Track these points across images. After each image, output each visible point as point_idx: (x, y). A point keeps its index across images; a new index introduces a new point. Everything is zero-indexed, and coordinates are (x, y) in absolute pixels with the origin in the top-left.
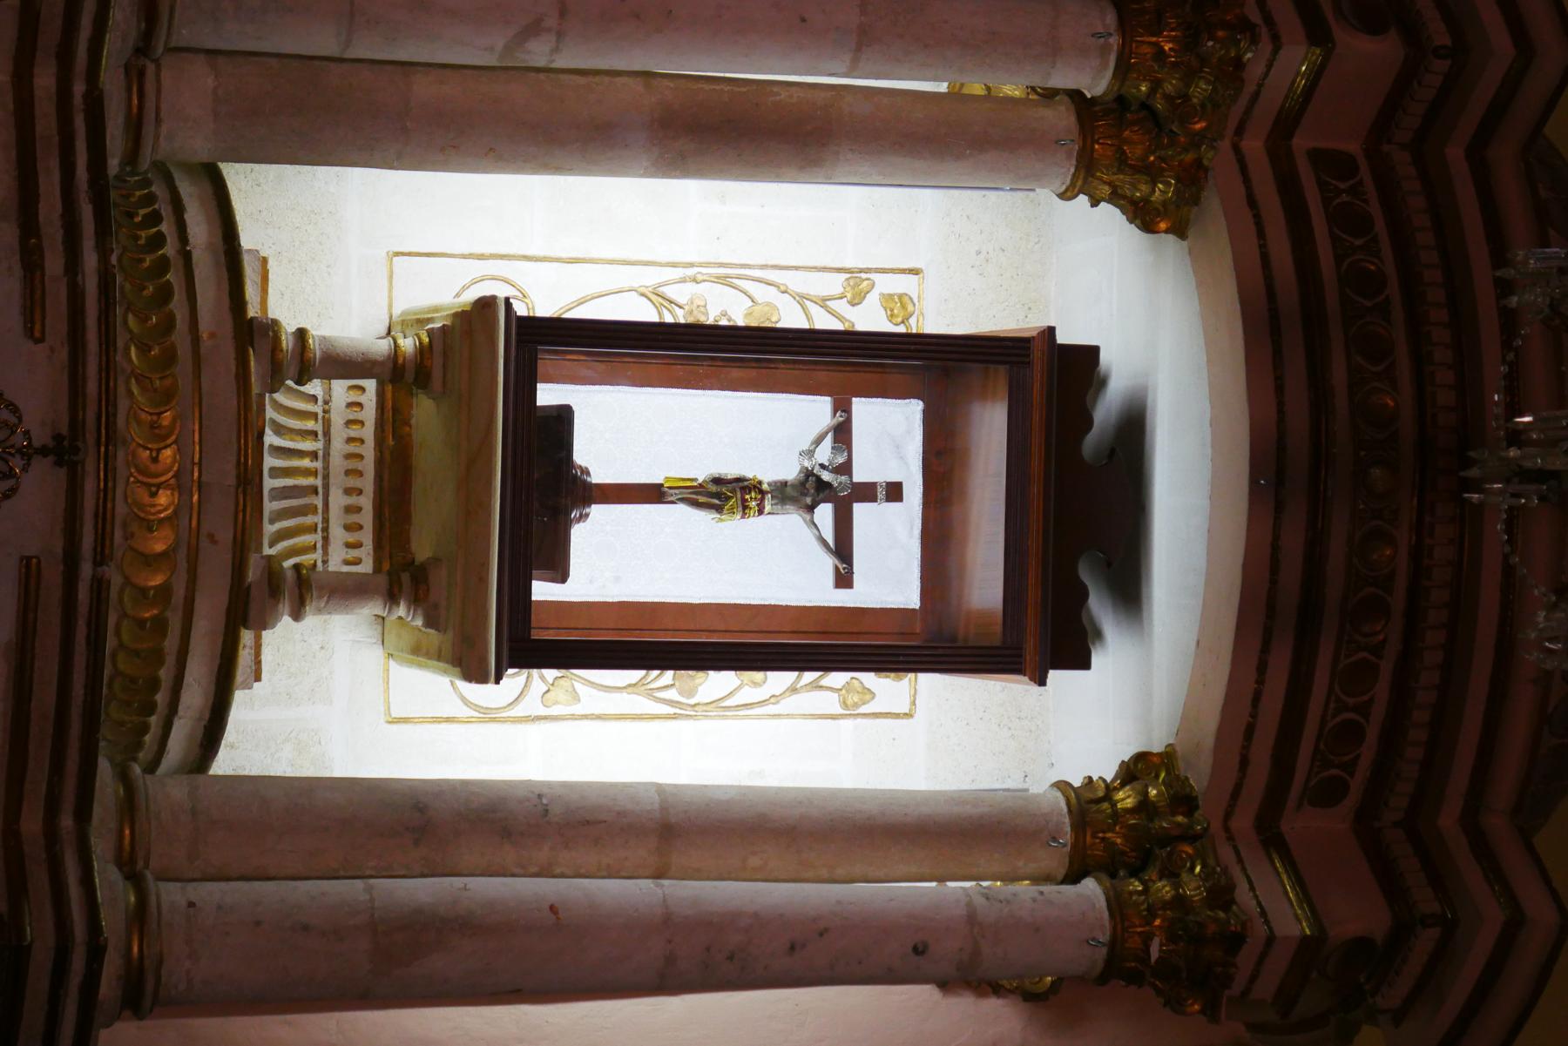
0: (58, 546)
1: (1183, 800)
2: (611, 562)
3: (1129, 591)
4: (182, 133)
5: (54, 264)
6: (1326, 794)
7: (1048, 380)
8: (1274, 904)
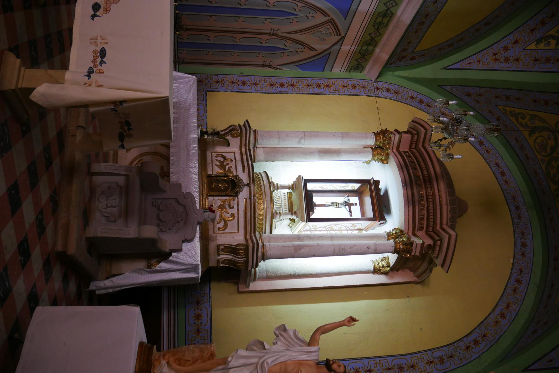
0: (249, 197)
1: (401, 231)
3: (389, 212)
5: (246, 165)
6: (421, 229)
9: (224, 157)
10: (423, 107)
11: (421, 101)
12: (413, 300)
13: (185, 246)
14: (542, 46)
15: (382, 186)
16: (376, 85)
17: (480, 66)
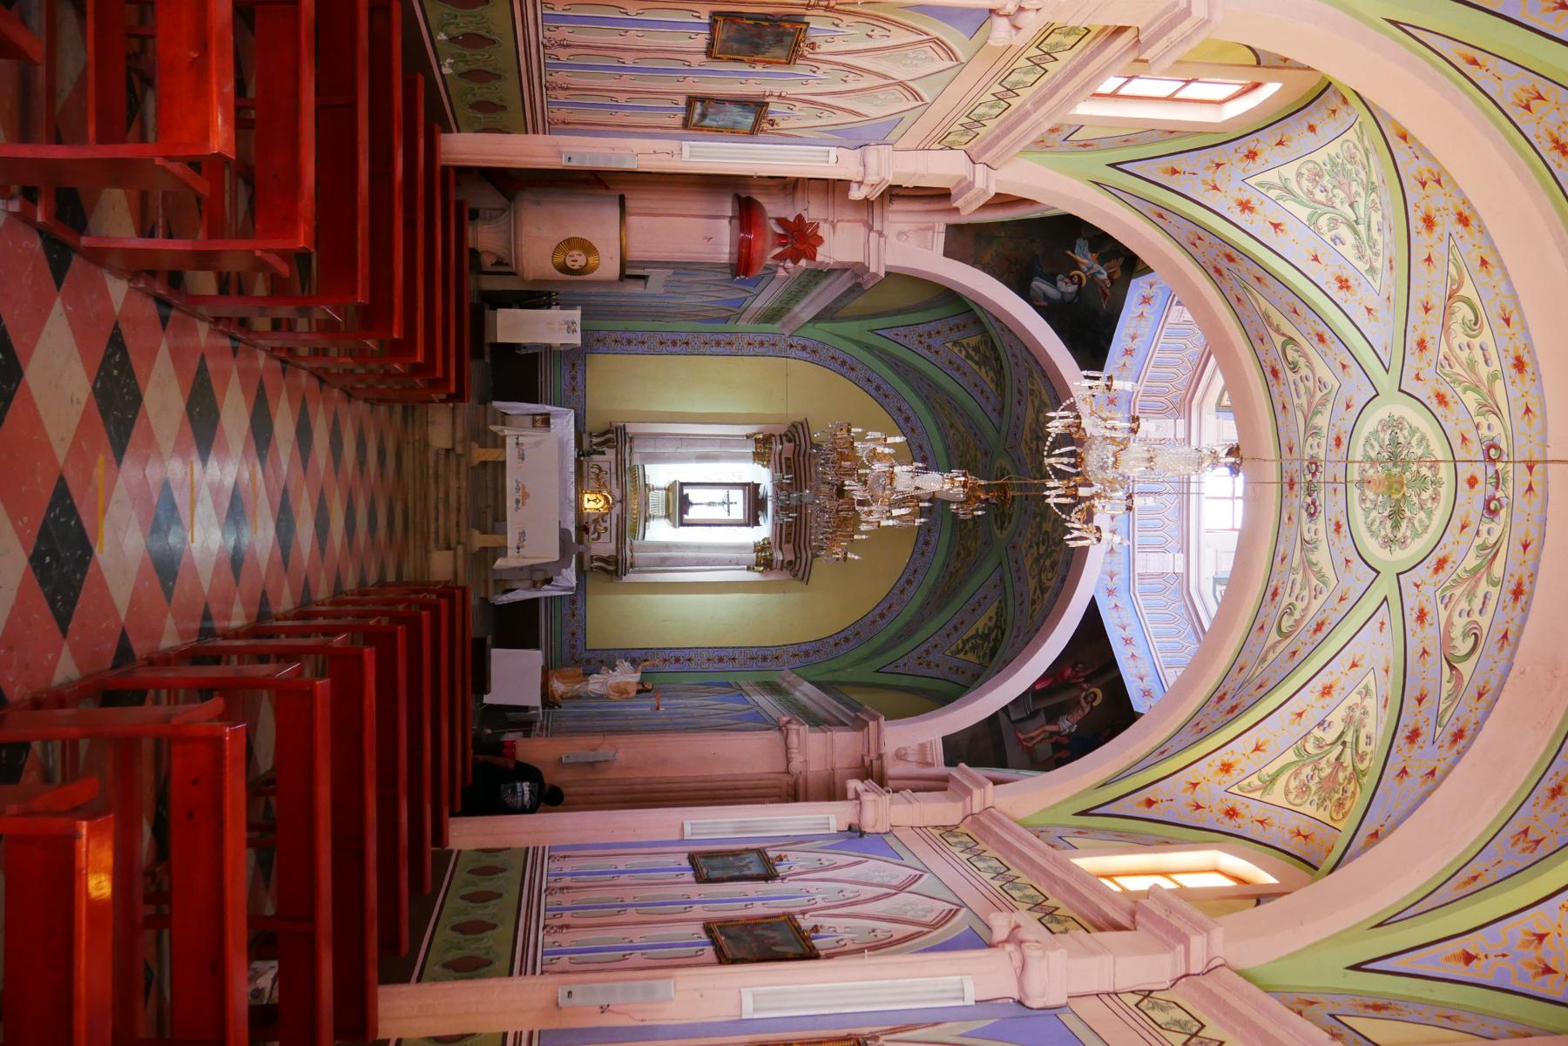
2: (693, 514)
4: (637, 461)
7: (752, 489)
8: (779, 556)
10: (844, 370)
11: (844, 363)
13: (564, 571)
14: (956, 350)
15: (761, 490)
16: (790, 341)
17: (906, 343)
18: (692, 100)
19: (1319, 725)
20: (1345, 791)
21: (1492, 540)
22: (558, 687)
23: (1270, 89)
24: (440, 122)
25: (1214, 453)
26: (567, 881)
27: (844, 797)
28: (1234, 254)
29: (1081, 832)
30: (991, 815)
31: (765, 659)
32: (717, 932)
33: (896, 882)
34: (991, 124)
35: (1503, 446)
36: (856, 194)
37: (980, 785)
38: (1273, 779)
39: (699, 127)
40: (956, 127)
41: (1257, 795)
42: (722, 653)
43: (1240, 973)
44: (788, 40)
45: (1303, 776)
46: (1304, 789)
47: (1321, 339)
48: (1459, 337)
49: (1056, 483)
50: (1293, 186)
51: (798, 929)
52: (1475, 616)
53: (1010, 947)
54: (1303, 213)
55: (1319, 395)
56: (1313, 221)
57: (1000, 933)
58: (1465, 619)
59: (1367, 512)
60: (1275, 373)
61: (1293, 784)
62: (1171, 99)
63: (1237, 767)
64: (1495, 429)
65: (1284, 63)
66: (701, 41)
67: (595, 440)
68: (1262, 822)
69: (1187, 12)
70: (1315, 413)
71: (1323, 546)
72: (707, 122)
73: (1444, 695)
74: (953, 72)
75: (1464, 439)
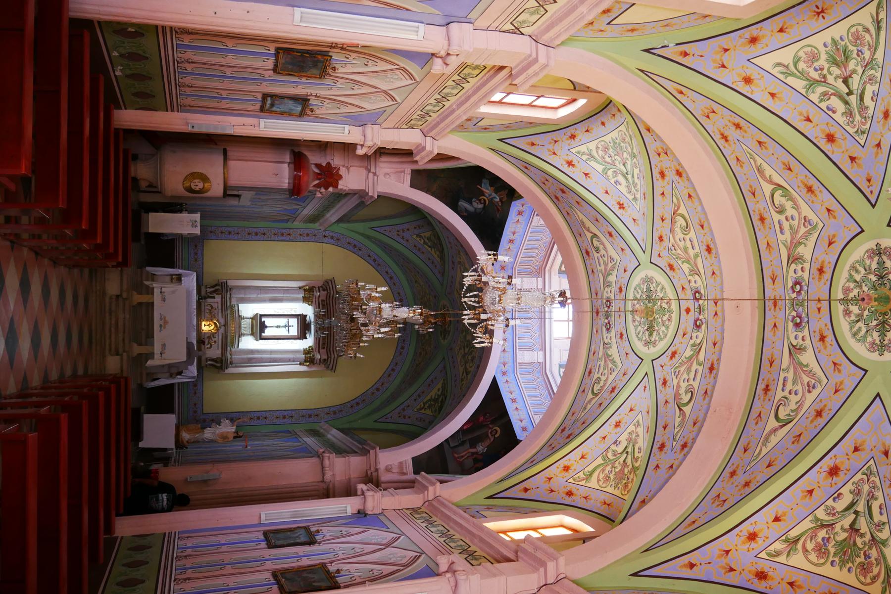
2: (268, 332)
4: (234, 302)
6: (323, 348)
7: (302, 318)
9: (212, 307)
11: (355, 246)
12: (323, 379)
15: (308, 318)
16: (324, 233)
17: (390, 235)
18: (265, 96)
19: (614, 443)
20: (628, 479)
21: (698, 341)
22: (185, 436)
23: (581, 102)
24: (114, 103)
25: (552, 295)
26: (189, 552)
27: (355, 494)
28: (565, 189)
29: (489, 508)
30: (439, 500)
31: (310, 416)
32: (280, 577)
33: (384, 542)
34: (434, 115)
35: (702, 292)
36: (360, 152)
37: (433, 484)
38: (591, 473)
39: (270, 111)
40: (415, 117)
41: (583, 483)
42: (285, 413)
43: (573, 581)
44: (320, 65)
45: (607, 472)
46: (607, 479)
47: (611, 235)
48: (679, 235)
49: (468, 312)
50: (594, 153)
51: (328, 572)
52: (691, 382)
53: (449, 575)
54: (600, 168)
55: (610, 265)
56: (605, 171)
57: (443, 567)
58: (686, 384)
59: (636, 327)
60: (587, 253)
61: (601, 476)
62: (530, 105)
63: (572, 468)
64: (698, 283)
65: (587, 90)
66: (270, 63)
67: (209, 290)
68: (585, 498)
69: (536, 60)
70: (609, 275)
71: (614, 346)
72: (274, 109)
73: (677, 425)
74: (412, 87)
75: (683, 288)
